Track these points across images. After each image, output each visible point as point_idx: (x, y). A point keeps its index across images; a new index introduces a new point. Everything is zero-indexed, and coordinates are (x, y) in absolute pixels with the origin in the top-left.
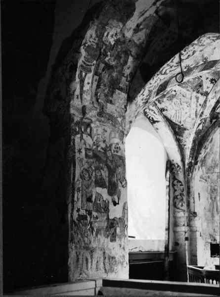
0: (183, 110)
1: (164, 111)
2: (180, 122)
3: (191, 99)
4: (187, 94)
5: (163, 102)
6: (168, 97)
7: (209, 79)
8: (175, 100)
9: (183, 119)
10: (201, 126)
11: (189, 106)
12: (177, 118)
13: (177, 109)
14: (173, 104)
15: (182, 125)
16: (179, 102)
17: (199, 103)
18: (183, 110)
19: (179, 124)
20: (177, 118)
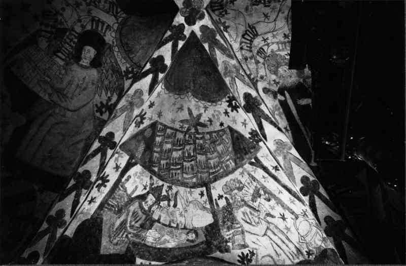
0: (273, 217)
1: (250, 261)
2: (299, 250)
3: (254, 179)
4: (240, 178)
5: (227, 242)
6: (224, 222)
7: (229, 110)
8: (239, 215)
9: (295, 238)
10: (319, 203)
11: (270, 196)
12: (284, 247)
13: (264, 226)
14: (247, 227)
15: (309, 253)
16: (248, 210)
17: (270, 169)
18: (273, 217)
19: (301, 258)
20: (284, 247)
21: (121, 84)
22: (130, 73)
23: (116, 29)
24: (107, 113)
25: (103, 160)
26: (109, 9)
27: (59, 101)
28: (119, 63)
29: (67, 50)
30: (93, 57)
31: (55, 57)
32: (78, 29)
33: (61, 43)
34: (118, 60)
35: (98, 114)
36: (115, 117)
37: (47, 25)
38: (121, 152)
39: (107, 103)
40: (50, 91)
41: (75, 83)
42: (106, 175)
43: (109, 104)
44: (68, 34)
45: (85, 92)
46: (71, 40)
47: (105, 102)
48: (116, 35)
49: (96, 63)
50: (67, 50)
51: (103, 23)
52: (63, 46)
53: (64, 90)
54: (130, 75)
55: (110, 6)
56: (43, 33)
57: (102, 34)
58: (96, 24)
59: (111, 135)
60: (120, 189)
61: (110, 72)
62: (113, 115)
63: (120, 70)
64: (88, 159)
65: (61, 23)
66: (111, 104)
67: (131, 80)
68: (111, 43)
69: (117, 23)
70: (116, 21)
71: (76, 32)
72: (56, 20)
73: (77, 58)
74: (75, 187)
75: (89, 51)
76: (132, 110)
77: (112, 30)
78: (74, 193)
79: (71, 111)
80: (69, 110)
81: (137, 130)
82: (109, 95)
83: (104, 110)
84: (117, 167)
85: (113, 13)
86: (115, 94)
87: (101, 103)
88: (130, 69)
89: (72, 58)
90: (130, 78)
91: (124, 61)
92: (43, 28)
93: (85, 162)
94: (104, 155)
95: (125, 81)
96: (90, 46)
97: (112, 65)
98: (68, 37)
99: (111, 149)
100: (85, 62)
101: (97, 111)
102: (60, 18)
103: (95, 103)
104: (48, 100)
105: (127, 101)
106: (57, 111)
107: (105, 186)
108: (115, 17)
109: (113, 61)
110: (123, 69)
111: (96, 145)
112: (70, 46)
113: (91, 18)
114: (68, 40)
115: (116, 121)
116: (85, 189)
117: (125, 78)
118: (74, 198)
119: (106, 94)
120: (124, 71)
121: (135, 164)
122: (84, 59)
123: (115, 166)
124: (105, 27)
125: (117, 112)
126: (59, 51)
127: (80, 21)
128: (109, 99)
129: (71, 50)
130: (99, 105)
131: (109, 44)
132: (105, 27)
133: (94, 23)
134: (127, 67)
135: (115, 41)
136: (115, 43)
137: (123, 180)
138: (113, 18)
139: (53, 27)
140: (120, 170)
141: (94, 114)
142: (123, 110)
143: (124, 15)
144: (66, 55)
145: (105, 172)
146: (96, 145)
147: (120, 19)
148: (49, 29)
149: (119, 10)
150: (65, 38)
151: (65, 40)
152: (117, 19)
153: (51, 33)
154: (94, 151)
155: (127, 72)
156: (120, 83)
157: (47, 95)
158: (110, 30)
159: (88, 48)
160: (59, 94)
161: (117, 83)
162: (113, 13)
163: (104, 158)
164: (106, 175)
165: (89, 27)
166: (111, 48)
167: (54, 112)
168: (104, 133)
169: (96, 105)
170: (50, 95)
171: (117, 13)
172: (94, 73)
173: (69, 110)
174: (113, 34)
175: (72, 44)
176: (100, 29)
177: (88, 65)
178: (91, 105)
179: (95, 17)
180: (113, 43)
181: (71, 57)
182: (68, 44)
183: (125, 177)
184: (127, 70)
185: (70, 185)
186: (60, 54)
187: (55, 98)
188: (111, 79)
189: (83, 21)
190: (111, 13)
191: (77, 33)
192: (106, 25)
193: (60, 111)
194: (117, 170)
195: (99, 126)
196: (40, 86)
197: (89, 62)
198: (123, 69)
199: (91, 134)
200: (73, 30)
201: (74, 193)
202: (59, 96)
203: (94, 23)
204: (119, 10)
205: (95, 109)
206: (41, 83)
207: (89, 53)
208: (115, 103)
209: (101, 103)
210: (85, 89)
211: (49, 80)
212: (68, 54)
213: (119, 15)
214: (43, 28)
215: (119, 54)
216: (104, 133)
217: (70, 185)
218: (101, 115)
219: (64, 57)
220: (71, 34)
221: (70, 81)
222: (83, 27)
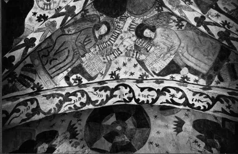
21: (166, 14)
22: (159, 8)
23: (134, 17)
24: (182, 22)
25: (212, 24)
26: (123, 21)
27: (175, 50)
28: (153, 15)
29: (146, 45)
30: (149, 31)
31: (150, 51)
32: (134, 38)
33: (143, 48)
34: (151, 16)
35: (183, 28)
36: (185, 17)
37: (133, 55)
38: (208, 13)
39: (177, 22)
40: (169, 55)
41: (165, 41)
42: (222, 23)
43: (177, 21)
44: (137, 44)
45: (170, 36)
46: (141, 42)
47: (176, 24)
48: (137, 17)
49: (153, 29)
50: (146, 45)
51: (131, 25)
52: (144, 47)
53: (168, 47)
54: (160, 8)
55: (122, 21)
56: (137, 57)
57: (137, 25)
58: (132, 29)
59: (196, 19)
60: (232, 14)
61: (158, 20)
62: (184, 18)
63: (157, 15)
64: (210, 33)
65: (132, 47)
66: (178, 20)
67: (163, 8)
68: (142, 20)
69: (130, 16)
70: (130, 17)
71: (136, 40)
72: (130, 50)
73: (150, 39)
74: (228, 41)
75: (146, 33)
76: (182, 6)
77: (134, 19)
78: (232, 41)
79: (180, 43)
80: (180, 45)
81: (194, 3)
82: (171, 21)
83: (180, 24)
84: (217, 16)
85: (125, 19)
86: (171, 18)
87: (176, 26)
88: (157, 8)
89: (151, 42)
90: (162, 9)
91: (152, 13)
92: (135, 56)
93: (213, 35)
94: (209, 23)
95: (164, 11)
96: (143, 32)
97: (155, 19)
98: (139, 44)
99: (205, 19)
100: (152, 35)
101: (181, 28)
102: (129, 48)
103: (176, 30)
104: (174, 55)
105: (176, 9)
106: (180, 51)
107: (229, 23)
108: (127, 18)
109: (152, 19)
110: (156, 12)
111: (202, 28)
112: (143, 43)
113: (128, 31)
114: (141, 44)
115: (188, 16)
116: (230, 34)
117: (162, 12)
118: (235, 42)
119: (171, 23)
120: (158, 12)
121: (216, 4)
122: (151, 36)
123: (216, 17)
124: (133, 24)
125: (182, 16)
126: (147, 49)
127: (130, 38)
128: (174, 21)
129: (146, 42)
130: (178, 27)
131: (142, 21)
132: (133, 24)
133: (131, 30)
134: (155, 11)
135: (140, 18)
136: (142, 18)
137: (226, 12)
138: (128, 19)
139: (134, 51)
140: (219, 14)
141: (182, 30)
142: (181, 12)
143: (126, 12)
144: (149, 45)
145: (220, 23)
146: (202, 28)
147: (129, 15)
148: (135, 54)
149: (123, 15)
150: (139, 45)
151: (140, 46)
152: (129, 17)
153: (137, 53)
154: (206, 29)
155: (158, 10)
156: (165, 15)
157: (171, 56)
158: (135, 21)
159: (145, 34)
160: (171, 50)
161: (165, 17)
162: (125, 19)
163: (210, 23)
164: (222, 23)
165: (134, 33)
166: (145, 21)
167: (180, 53)
168: (195, 24)
169: (178, 29)
170: (171, 55)
171: (125, 17)
172: (159, 30)
173: (180, 45)
174: (137, 19)
175: (143, 42)
176: (134, 27)
177: (154, 33)
178: (177, 32)
179: (128, 29)
180: (142, 19)
181: (149, 43)
182: (142, 44)
183: (224, 10)
184: (157, 11)
185: (227, 44)
186: (148, 49)
187: (173, 52)
188: (163, 20)
189: (130, 36)
190: (125, 20)
191: (137, 39)
192: (132, 23)
193: (180, 49)
194: (219, 16)
195: (190, 26)
196: (166, 60)
197: (152, 33)
198: (156, 12)
199: (195, 32)
200: (135, 41)
201: (232, 41)
202: (172, 50)
203: (131, 30)
204: (123, 15)
205: (180, 29)
206: (164, 59)
207: (147, 33)
208: (177, 17)
209: (176, 26)
210: (168, 36)
211: (162, 55)
212: (149, 44)
213: (126, 15)
214: (135, 56)
215: (148, 15)
216: (195, 24)
217: (227, 44)
218: (183, 26)
219: (150, 47)
220: (137, 42)
221: (163, 44)
222: (133, 36)
